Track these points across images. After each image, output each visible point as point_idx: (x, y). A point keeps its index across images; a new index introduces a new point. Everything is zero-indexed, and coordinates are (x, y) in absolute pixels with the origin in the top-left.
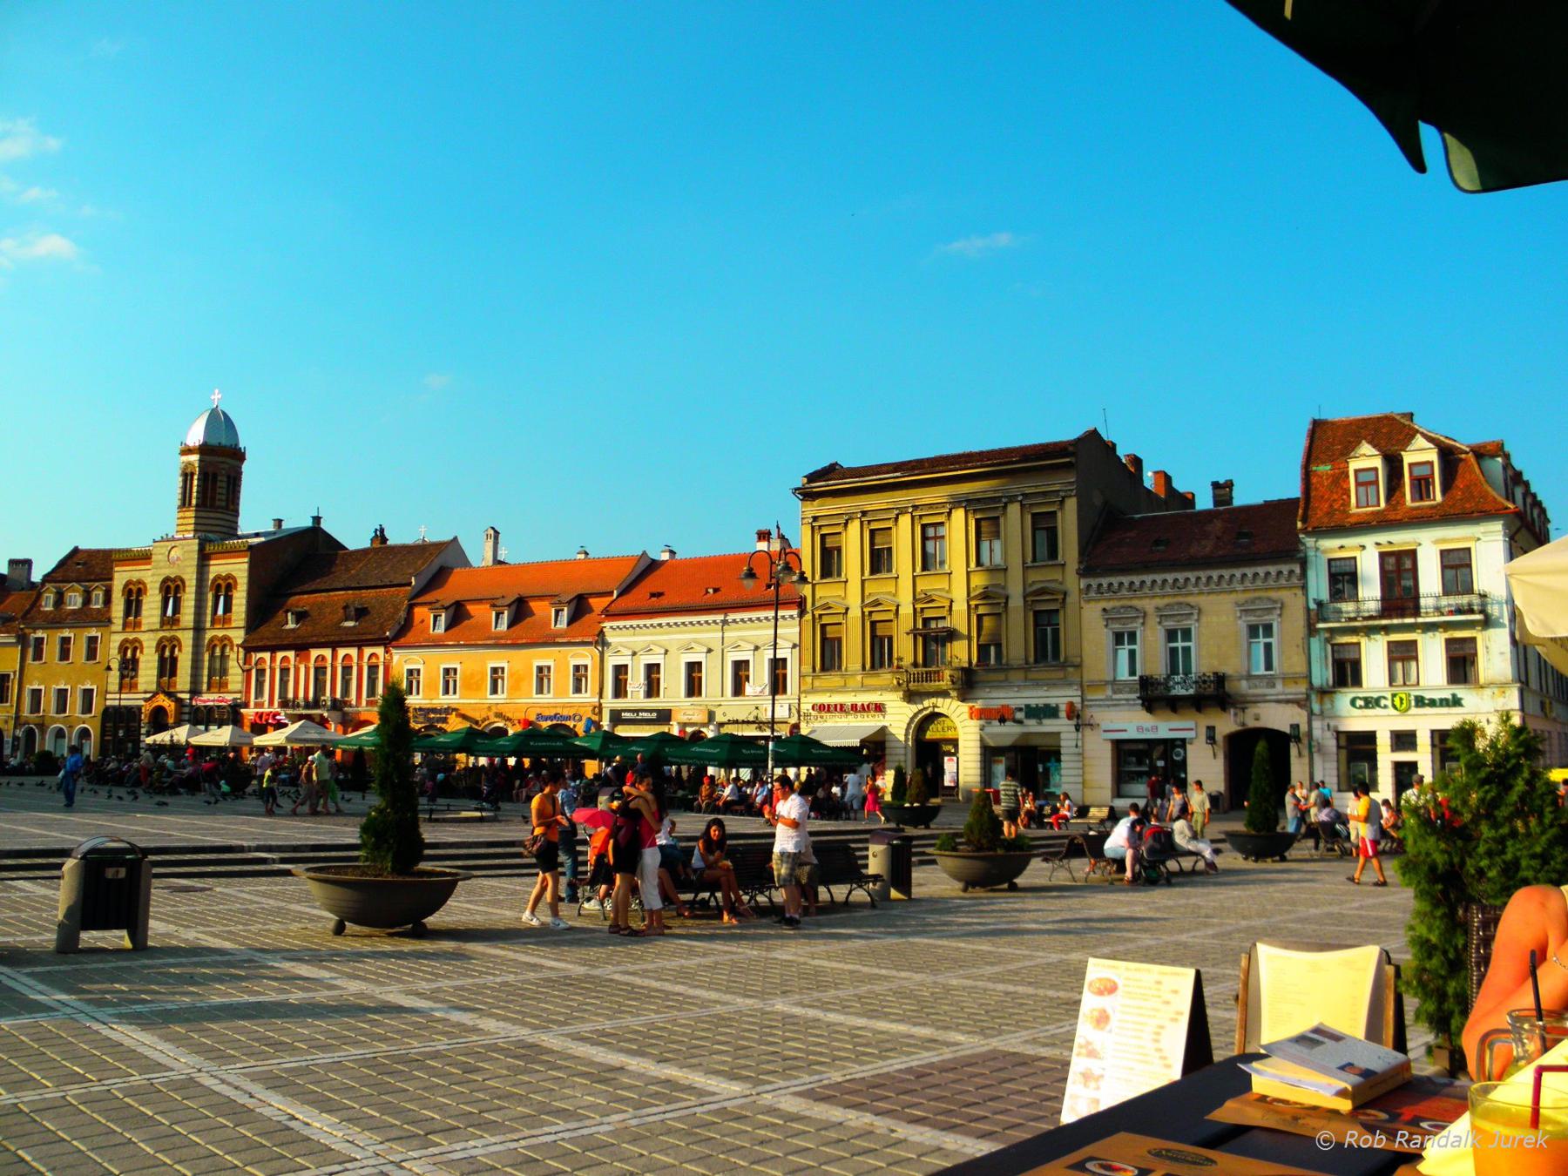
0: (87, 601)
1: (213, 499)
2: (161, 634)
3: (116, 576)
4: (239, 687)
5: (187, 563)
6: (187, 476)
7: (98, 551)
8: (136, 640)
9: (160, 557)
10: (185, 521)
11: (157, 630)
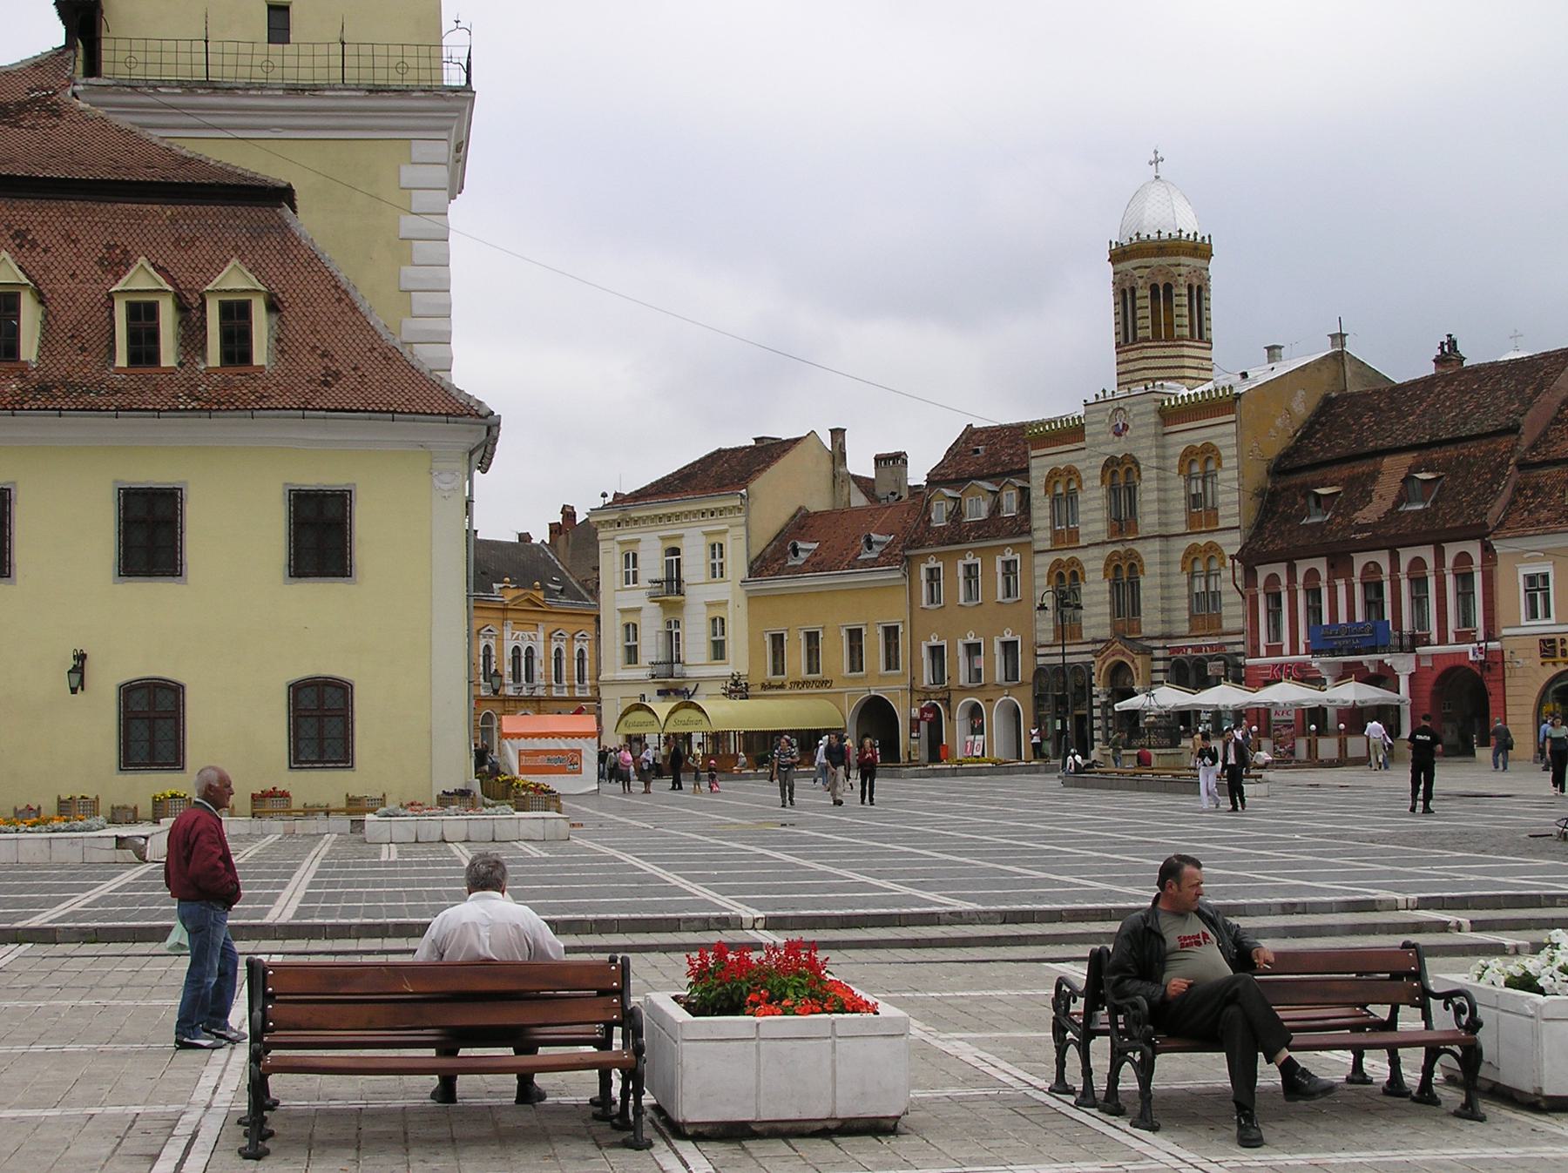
0: (996, 508)
1: (1170, 325)
2: (1110, 549)
3: (1033, 463)
4: (1239, 624)
5: (1141, 432)
6: (1125, 295)
7: (1002, 428)
8: (1073, 561)
9: (1098, 427)
10: (1130, 366)
11: (1104, 543)
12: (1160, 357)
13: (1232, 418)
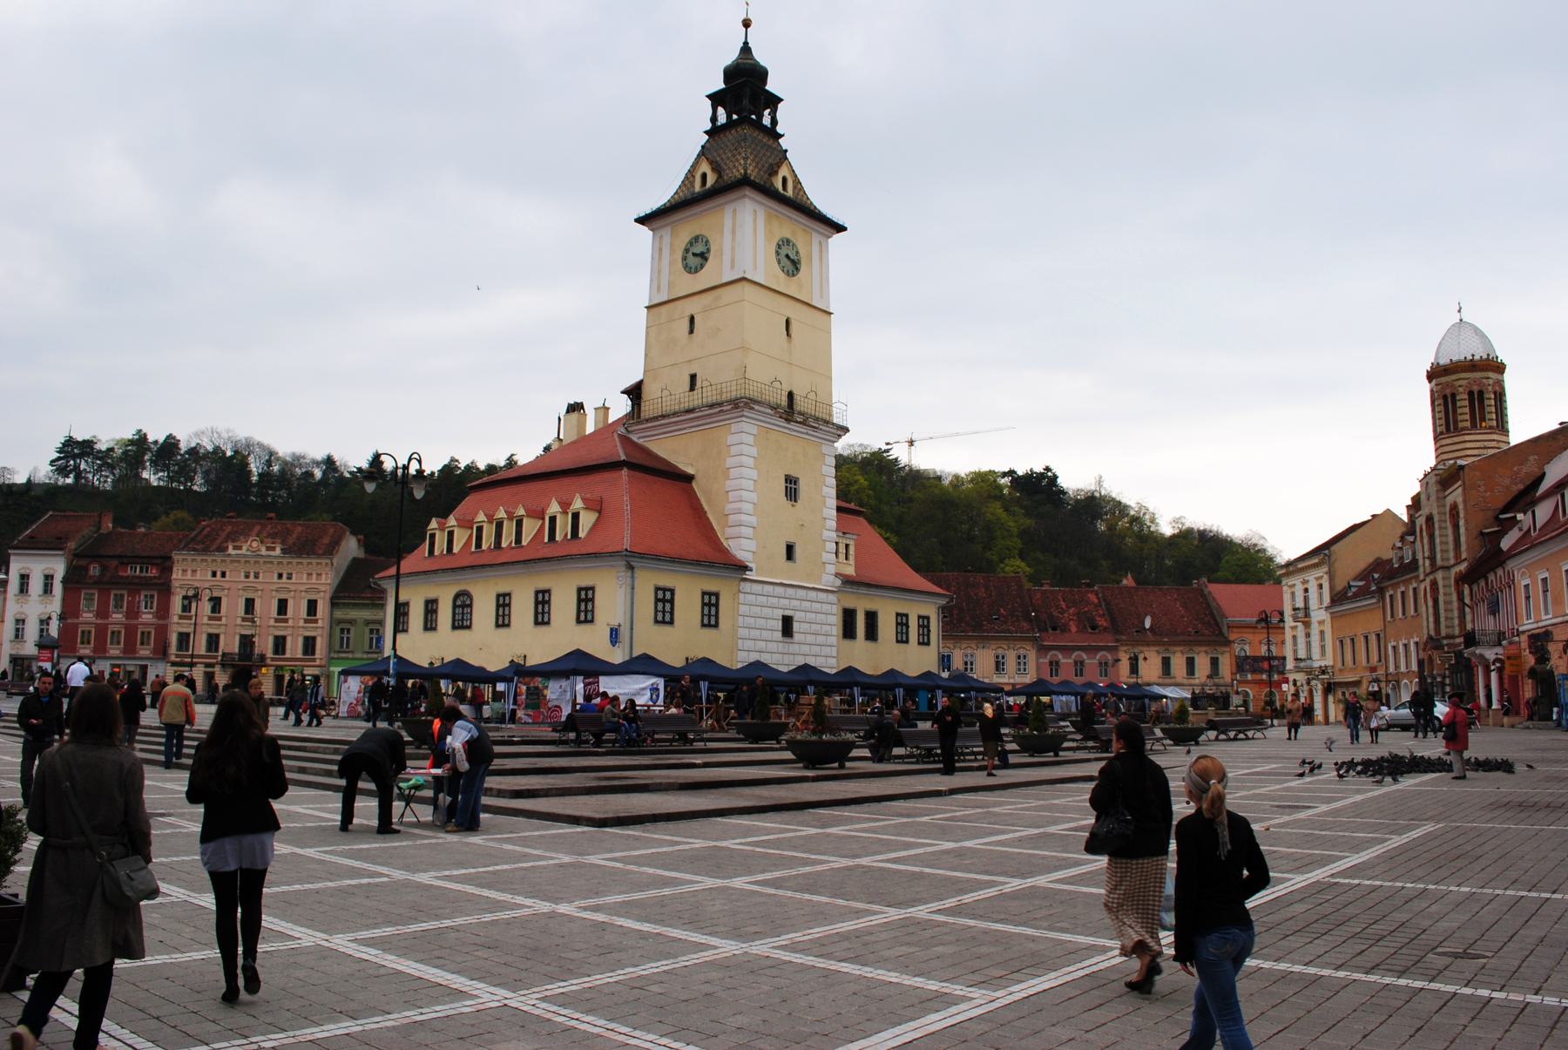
1: (1456, 422)
12: (1451, 444)
13: (1460, 483)
